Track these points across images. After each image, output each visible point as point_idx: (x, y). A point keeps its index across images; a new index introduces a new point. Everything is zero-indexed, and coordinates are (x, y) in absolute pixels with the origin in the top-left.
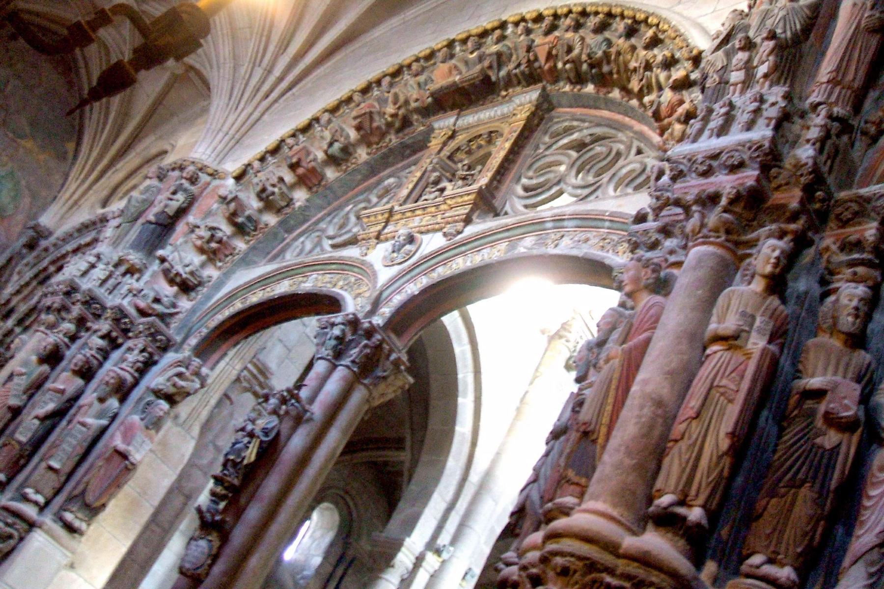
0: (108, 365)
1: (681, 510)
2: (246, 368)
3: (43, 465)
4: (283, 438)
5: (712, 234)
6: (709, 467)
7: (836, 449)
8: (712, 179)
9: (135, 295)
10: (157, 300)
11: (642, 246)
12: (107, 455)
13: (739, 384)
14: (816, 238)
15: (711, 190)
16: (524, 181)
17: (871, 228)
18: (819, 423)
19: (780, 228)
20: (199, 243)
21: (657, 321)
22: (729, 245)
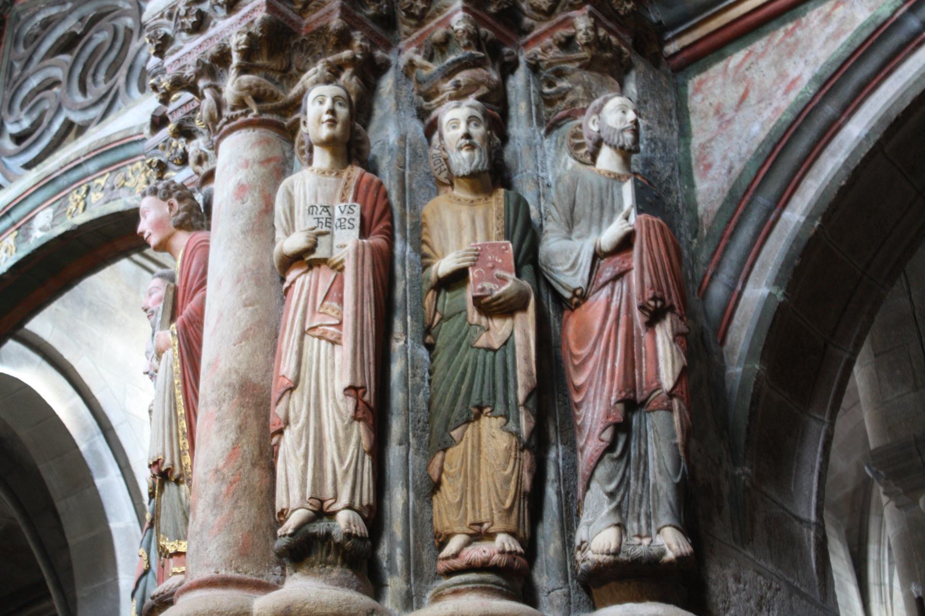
1: (320, 527)
5: (239, 112)
6: (339, 449)
7: (508, 343)
8: (211, 32)
11: (171, 165)
13: (340, 313)
14: (392, 57)
15: (213, 49)
16: (12, 129)
17: (456, 12)
18: (474, 316)
19: (329, 63)
21: (205, 273)
22: (266, 117)
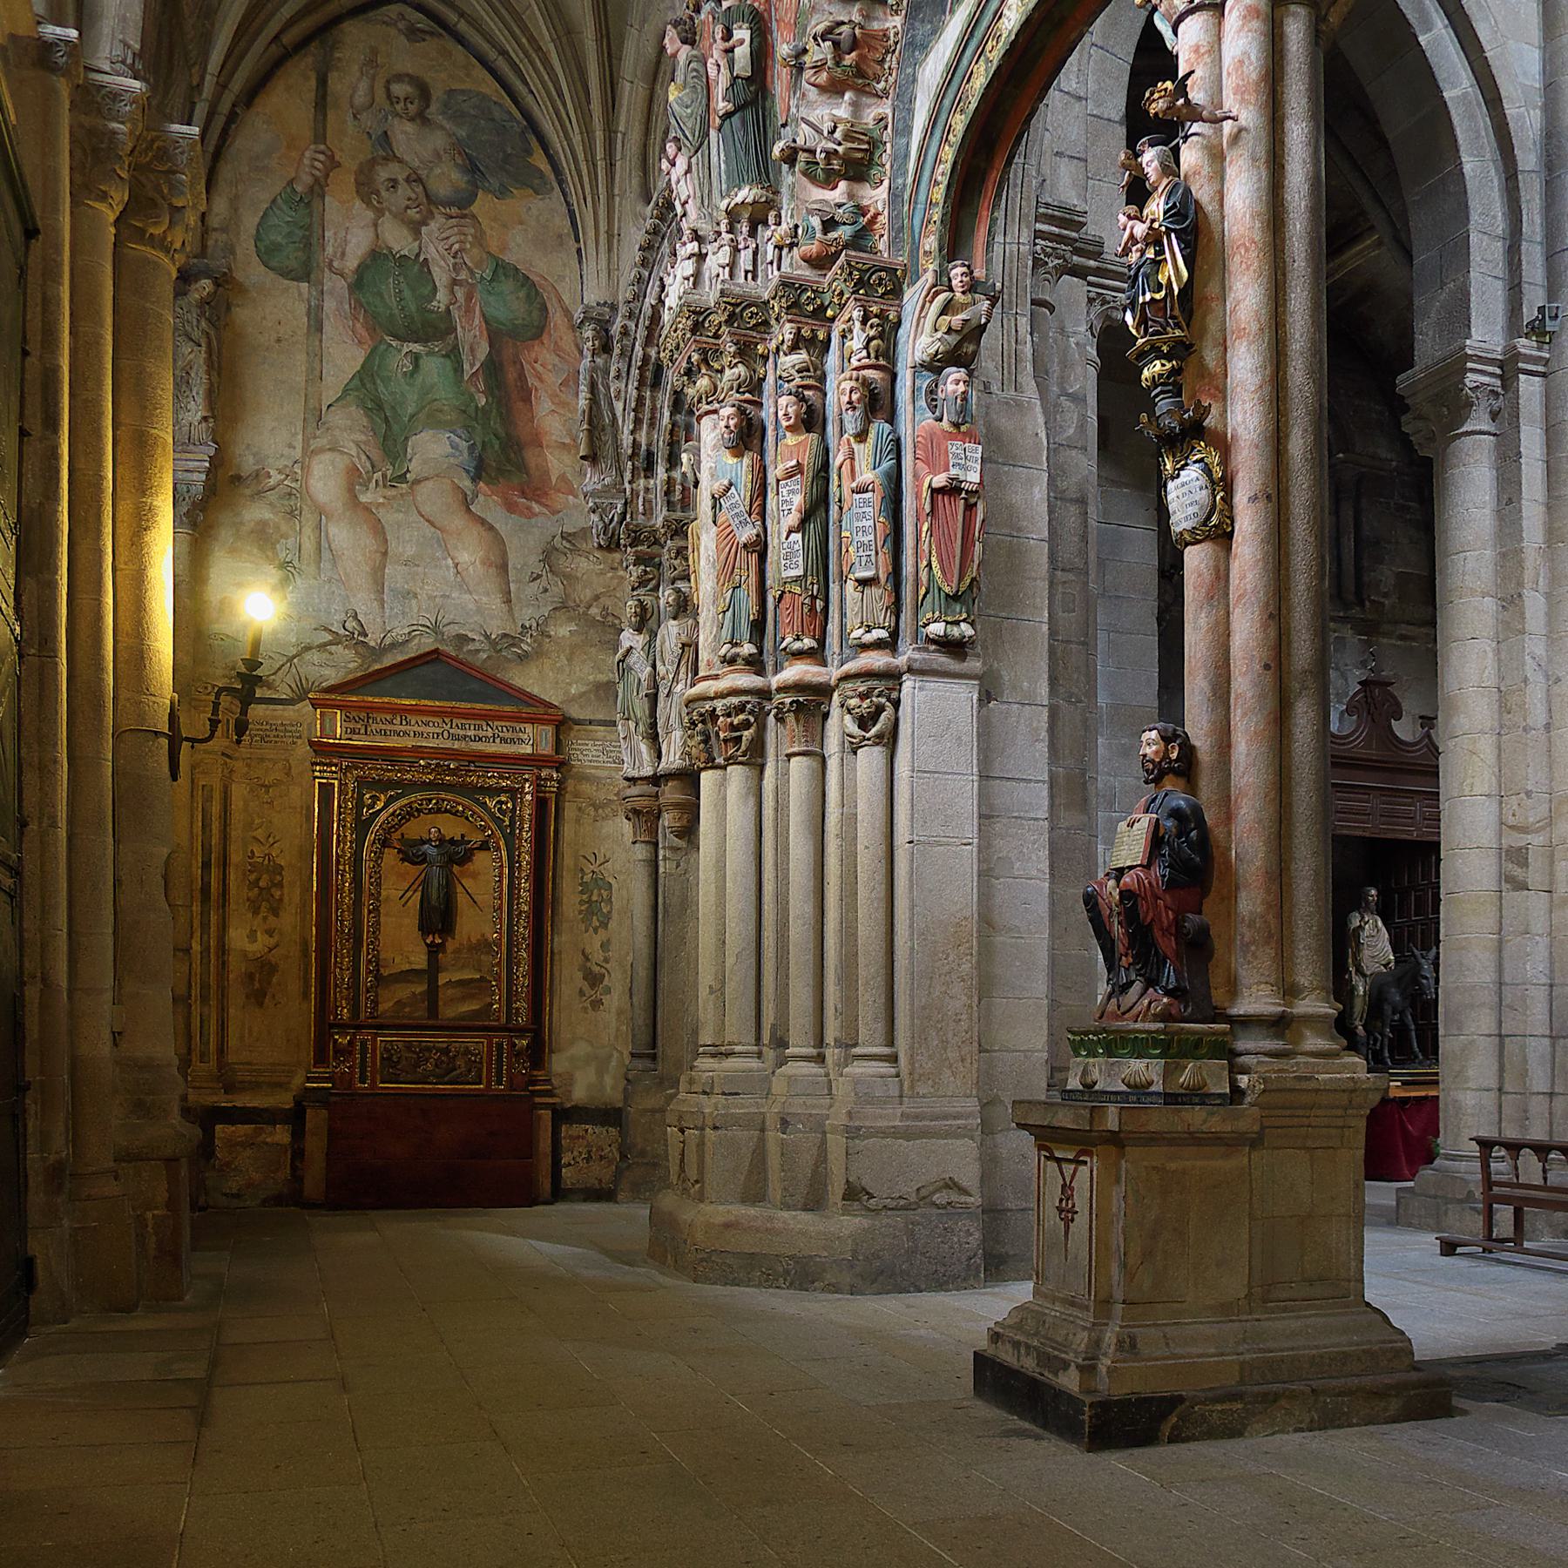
0: (830, 385)
2: (1038, 234)
3: (850, 585)
4: (1210, 207)
9: (791, 246)
10: (829, 224)
12: (927, 508)
20: (823, 77)
